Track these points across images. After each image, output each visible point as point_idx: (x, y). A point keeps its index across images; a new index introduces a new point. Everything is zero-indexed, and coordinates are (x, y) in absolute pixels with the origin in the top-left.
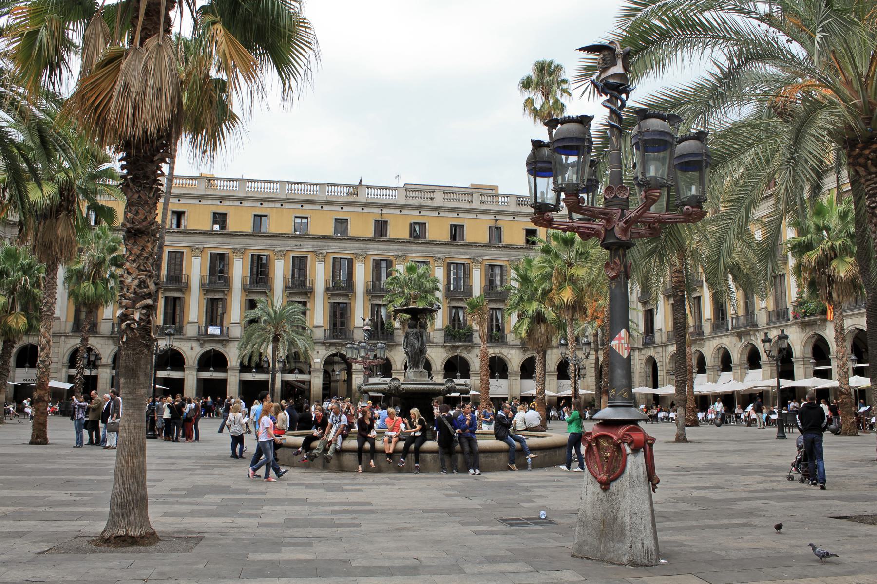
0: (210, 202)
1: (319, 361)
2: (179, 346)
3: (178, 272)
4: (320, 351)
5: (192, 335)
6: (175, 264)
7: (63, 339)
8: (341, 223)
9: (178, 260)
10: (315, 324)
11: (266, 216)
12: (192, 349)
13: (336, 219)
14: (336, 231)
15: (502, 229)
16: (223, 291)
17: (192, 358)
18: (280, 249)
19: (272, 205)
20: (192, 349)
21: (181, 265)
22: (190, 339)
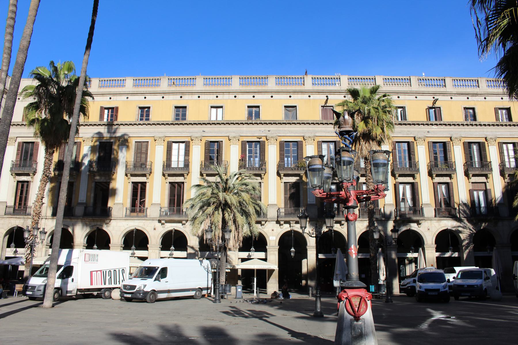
0: (171, 97)
1: (274, 238)
2: (143, 227)
3: (143, 160)
4: (275, 229)
6: (141, 153)
8: (290, 108)
9: (144, 150)
10: (270, 203)
11: (222, 107)
13: (285, 107)
14: (286, 116)
15: (442, 109)
16: (182, 175)
18: (235, 135)
19: (226, 96)
20: (155, 229)
21: (147, 154)
22: (153, 219)
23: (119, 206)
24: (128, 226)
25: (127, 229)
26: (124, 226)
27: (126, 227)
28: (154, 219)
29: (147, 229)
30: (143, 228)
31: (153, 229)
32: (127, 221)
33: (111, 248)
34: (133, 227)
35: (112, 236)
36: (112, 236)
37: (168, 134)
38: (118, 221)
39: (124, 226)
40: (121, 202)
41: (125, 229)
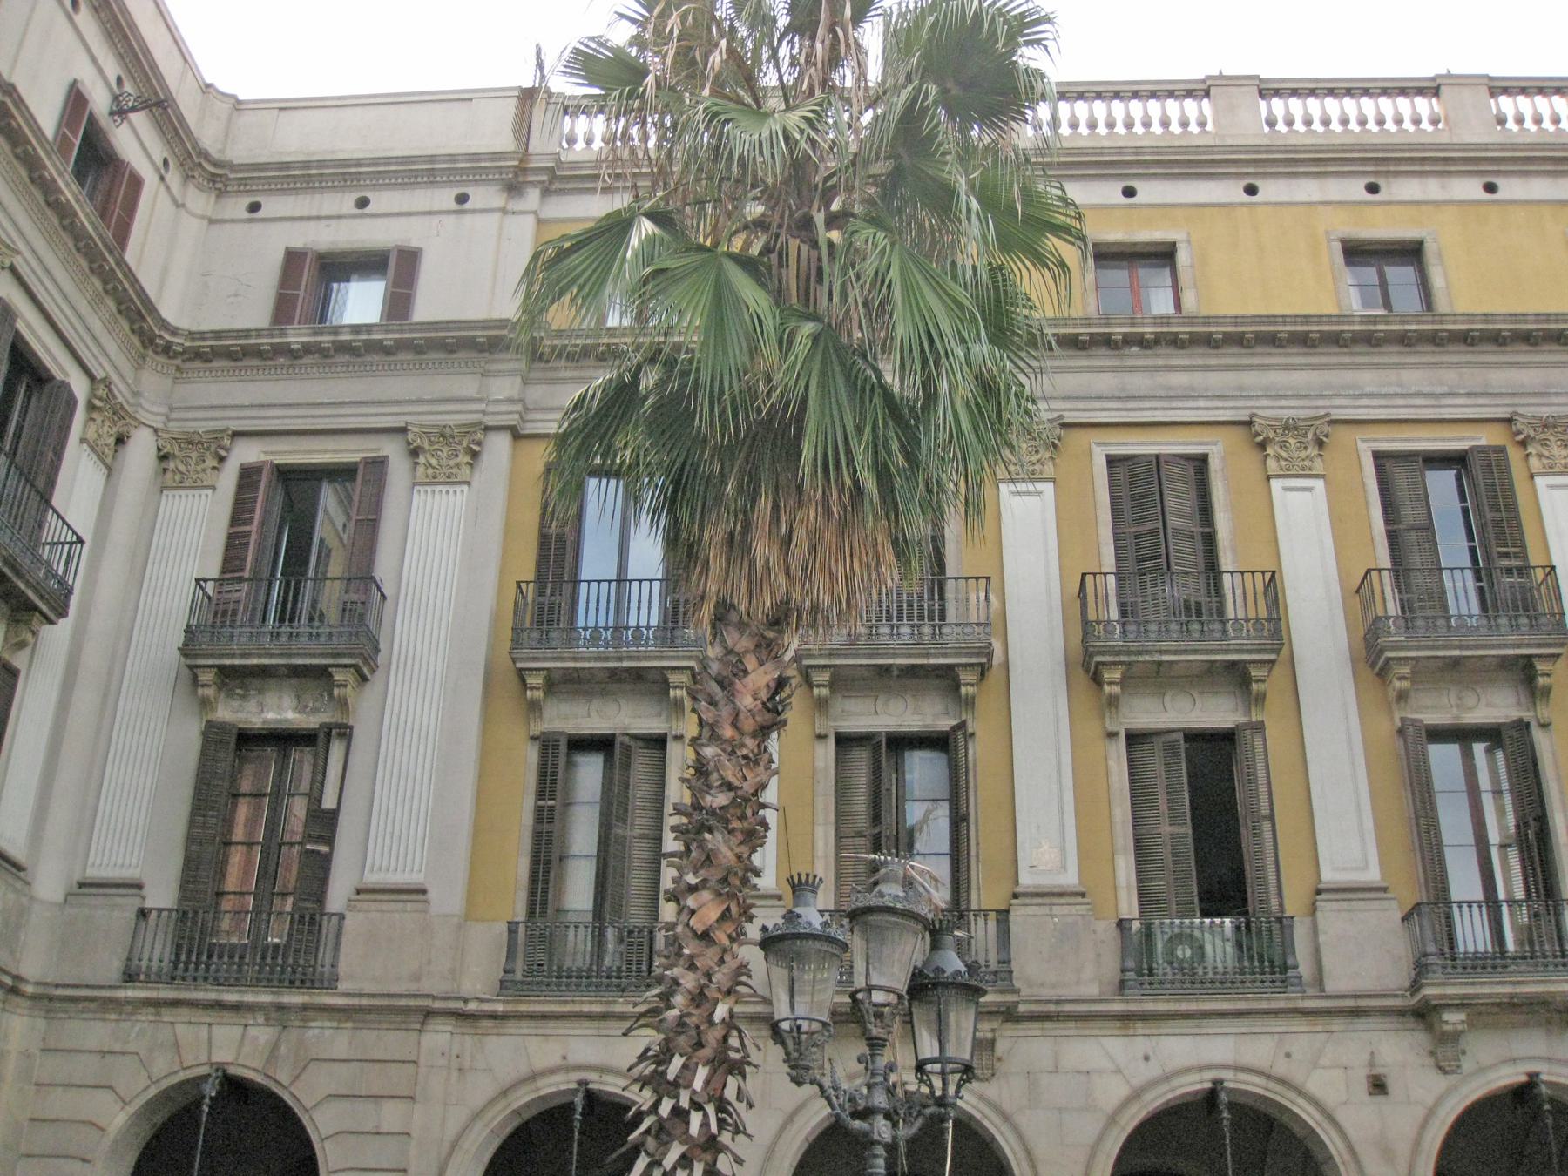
2: (1281, 1069)
5: (1366, 984)
12: (1378, 1086)
17: (1388, 1155)
20: (1378, 1086)
22: (1355, 1012)
24: (1153, 1071)
25: (1148, 1097)
26: (1118, 1071)
28: (1364, 1003)
29: (1313, 1085)
30: (1282, 1081)
31: (1362, 1086)
32: (1140, 1028)
34: (1195, 1077)
35: (1028, 1153)
36: (1028, 1153)
37: (1338, 402)
39: (1118, 1071)
41: (1136, 1095)
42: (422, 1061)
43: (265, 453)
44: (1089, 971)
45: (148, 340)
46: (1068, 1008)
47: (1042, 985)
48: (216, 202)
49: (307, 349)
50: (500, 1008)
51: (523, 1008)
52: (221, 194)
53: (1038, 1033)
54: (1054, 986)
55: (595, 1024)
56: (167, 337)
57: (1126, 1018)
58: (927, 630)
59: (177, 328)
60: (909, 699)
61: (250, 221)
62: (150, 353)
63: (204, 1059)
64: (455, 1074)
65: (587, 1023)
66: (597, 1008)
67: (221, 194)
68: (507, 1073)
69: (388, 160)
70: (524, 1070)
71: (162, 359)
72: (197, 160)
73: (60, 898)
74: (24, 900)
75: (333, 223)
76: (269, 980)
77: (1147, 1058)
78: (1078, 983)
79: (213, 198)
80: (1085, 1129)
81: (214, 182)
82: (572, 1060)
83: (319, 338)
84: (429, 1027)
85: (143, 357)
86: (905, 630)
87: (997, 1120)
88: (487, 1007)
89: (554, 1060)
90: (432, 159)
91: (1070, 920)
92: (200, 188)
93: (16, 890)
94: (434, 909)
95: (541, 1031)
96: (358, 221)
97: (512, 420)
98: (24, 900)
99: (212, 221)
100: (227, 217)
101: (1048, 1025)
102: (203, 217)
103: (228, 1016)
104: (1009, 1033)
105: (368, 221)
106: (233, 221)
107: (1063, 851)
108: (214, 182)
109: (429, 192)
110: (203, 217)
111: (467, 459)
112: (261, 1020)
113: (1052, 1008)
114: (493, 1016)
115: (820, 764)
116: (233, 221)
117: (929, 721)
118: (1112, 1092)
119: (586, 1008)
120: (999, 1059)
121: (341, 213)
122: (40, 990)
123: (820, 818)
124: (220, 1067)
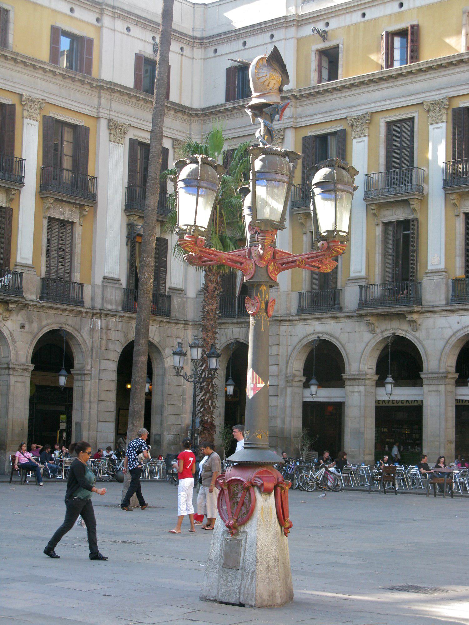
7: (285, 327)
23: (435, 277)
27: (456, 327)
32: (457, 313)
33: (425, 382)
38: (437, 315)
40: (442, 266)
41: (455, 334)
42: (281, 334)
43: (230, 146)
44: (443, 297)
45: (190, 115)
46: (436, 309)
47: (430, 302)
48: (205, 51)
49: (234, 108)
50: (297, 318)
51: (303, 317)
52: (205, 48)
53: (430, 316)
54: (433, 302)
55: (320, 320)
56: (194, 112)
57: (453, 311)
58: (398, 189)
59: (197, 109)
60: (401, 209)
61: (215, 57)
62: (192, 118)
63: (232, 338)
64: (289, 337)
65: (318, 320)
66: (319, 316)
67: (205, 48)
68: (300, 336)
69: (247, 27)
70: (305, 335)
71: (196, 119)
72: (193, 41)
73: (194, 296)
74: (185, 299)
75: (238, 53)
76: (241, 315)
77: (458, 323)
78: (440, 300)
79: (203, 50)
80: (440, 344)
81: (202, 45)
82: (316, 331)
83: (234, 105)
84: (282, 325)
85: (191, 120)
86: (392, 189)
87: (418, 343)
88: (294, 318)
89: (312, 331)
90: (260, 24)
91: (438, 280)
92: (198, 48)
93: (181, 297)
94: (281, 290)
95: (308, 323)
96: (244, 51)
97: (292, 124)
98: (185, 299)
99: (205, 59)
100: (209, 57)
101: (432, 314)
102: (201, 59)
103: (236, 326)
104: (422, 317)
105: (247, 51)
106: (210, 58)
107: (440, 257)
108: (202, 45)
109: (262, 35)
110: (201, 59)
111: (280, 141)
112: (243, 325)
113: (431, 309)
114: (296, 320)
115: (377, 234)
116: (210, 58)
117: (406, 215)
118: (448, 333)
119: (317, 316)
120: (419, 325)
121: (239, 49)
122: (193, 323)
123: (377, 252)
124: (236, 340)
